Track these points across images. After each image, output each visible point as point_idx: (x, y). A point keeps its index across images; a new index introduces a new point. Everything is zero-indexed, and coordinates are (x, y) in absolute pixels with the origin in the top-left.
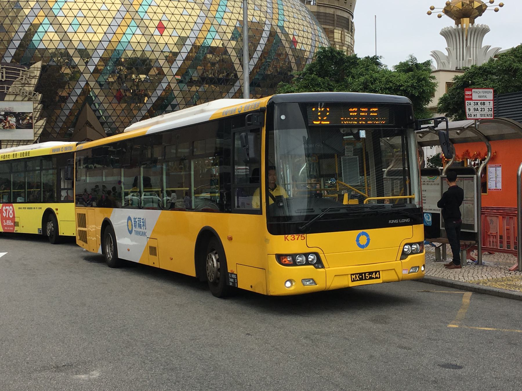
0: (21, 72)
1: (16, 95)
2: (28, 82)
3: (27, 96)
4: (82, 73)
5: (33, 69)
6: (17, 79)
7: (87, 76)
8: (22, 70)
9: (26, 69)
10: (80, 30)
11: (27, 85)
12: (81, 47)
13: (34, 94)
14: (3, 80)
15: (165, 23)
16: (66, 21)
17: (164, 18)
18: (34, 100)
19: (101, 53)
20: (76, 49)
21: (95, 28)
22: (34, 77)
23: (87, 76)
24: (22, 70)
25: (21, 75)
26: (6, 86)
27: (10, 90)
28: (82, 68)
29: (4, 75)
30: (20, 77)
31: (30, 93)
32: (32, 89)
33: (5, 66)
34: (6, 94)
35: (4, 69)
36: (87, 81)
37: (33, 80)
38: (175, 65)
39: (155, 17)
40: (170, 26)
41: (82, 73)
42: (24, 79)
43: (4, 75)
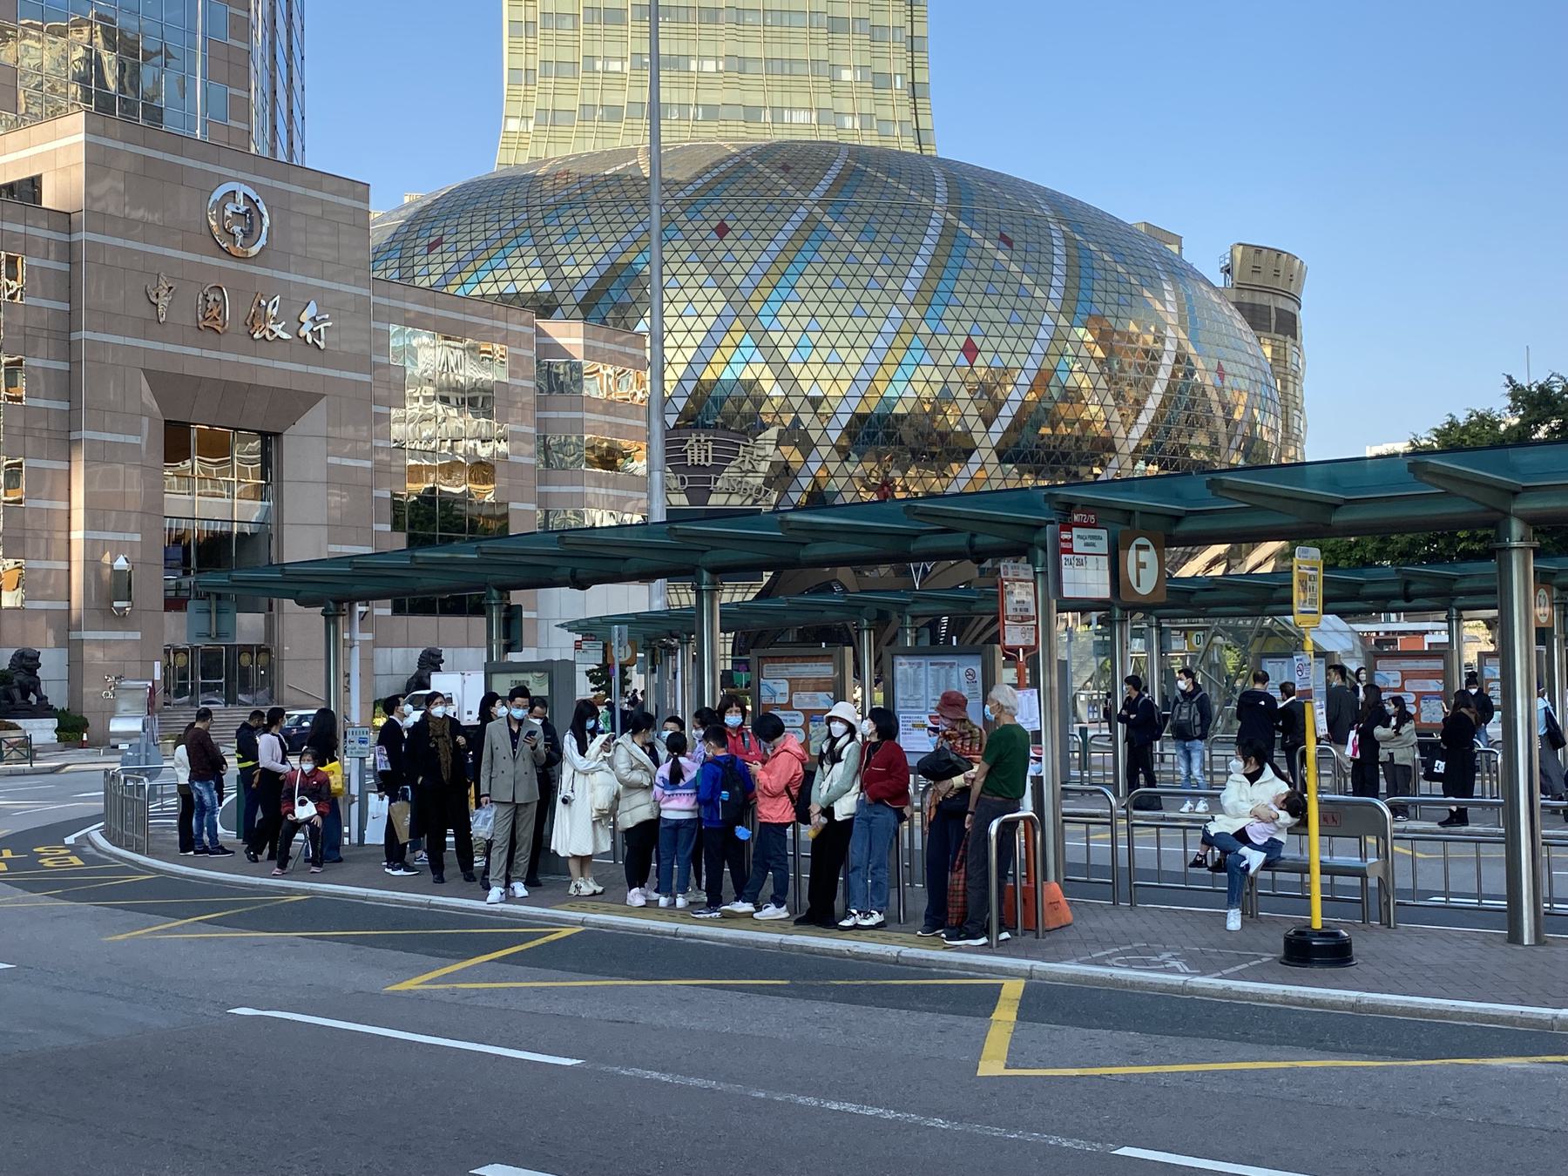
0: (742, 447)
1: (731, 493)
2: (754, 467)
3: (750, 495)
4: (815, 445)
5: (763, 442)
6: (732, 463)
7: (824, 451)
8: (744, 445)
9: (751, 441)
10: (815, 357)
11: (751, 474)
12: (815, 392)
13: (766, 492)
14: (708, 464)
15: (977, 341)
16: (786, 341)
17: (976, 330)
18: (764, 503)
19: (854, 403)
20: (806, 396)
21: (843, 353)
22: (764, 458)
23: (824, 451)
24: (744, 445)
25: (740, 454)
26: (713, 476)
27: (718, 484)
28: (814, 436)
29: (710, 455)
30: (741, 459)
31: (759, 491)
32: (760, 481)
33: (711, 438)
34: (711, 492)
35: (710, 443)
36: (824, 461)
37: (763, 463)
38: (995, 427)
39: (958, 330)
40: (986, 346)
41: (815, 445)
42: (747, 462)
43: (710, 455)
